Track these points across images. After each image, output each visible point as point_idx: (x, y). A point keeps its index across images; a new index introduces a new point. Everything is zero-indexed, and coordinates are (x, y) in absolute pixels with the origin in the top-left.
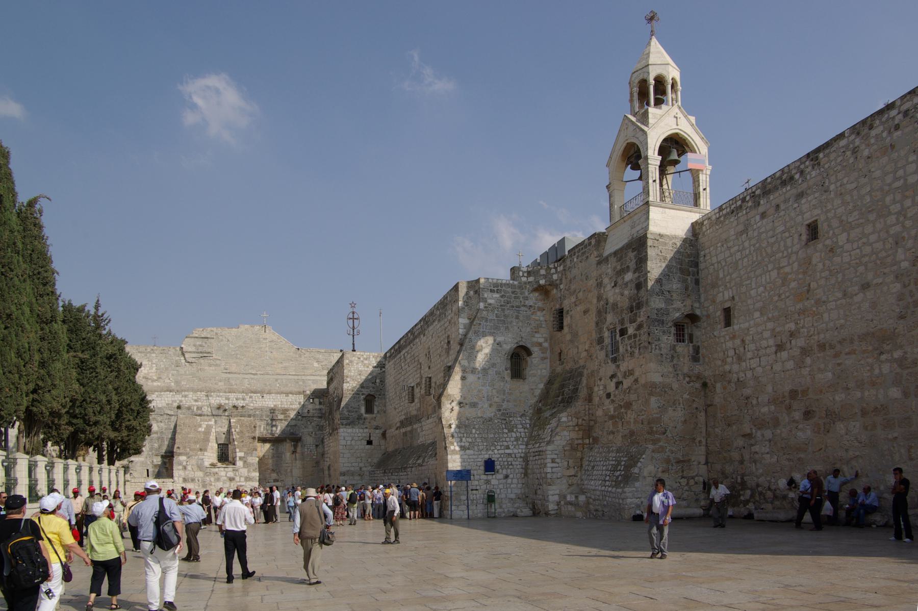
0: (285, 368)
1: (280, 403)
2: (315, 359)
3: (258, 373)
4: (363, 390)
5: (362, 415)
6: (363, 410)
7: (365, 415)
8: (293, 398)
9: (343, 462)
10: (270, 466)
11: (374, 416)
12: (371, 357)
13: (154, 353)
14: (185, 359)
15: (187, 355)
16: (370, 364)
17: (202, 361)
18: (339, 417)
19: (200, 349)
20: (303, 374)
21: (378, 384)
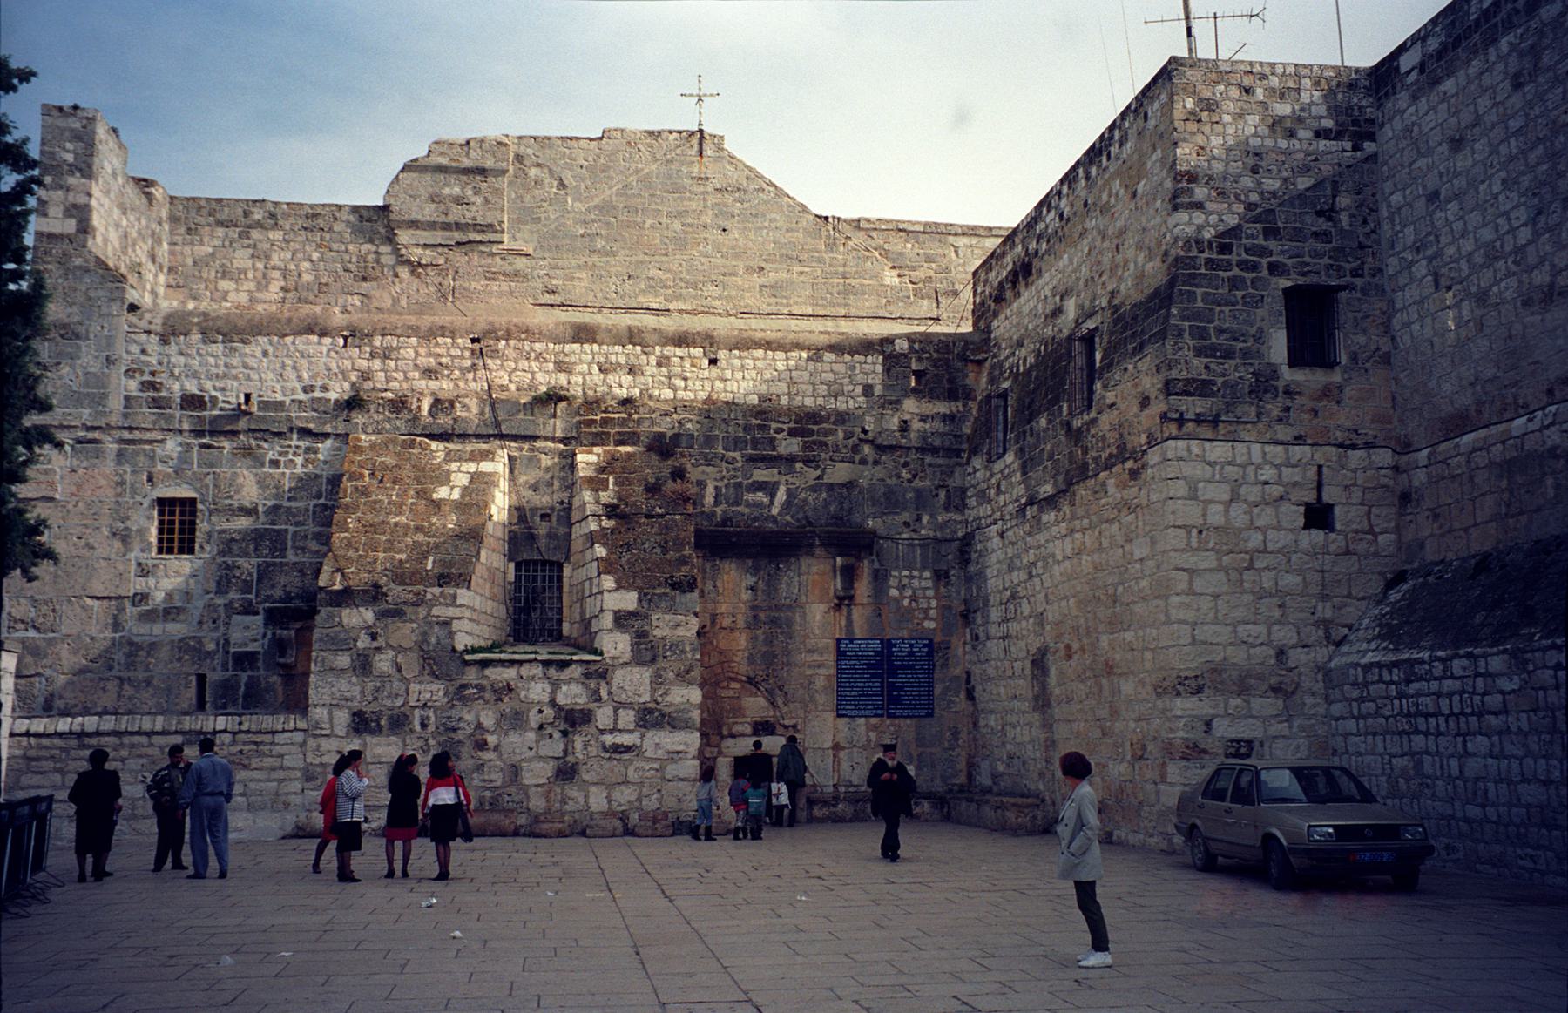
0: (775, 289)
1: (783, 387)
2: (886, 254)
3: (671, 307)
4: (1272, 245)
5: (1275, 373)
6: (1278, 346)
7: (1288, 375)
8: (839, 368)
9: (1190, 615)
10: (741, 666)
11: (1336, 377)
12: (1307, 82)
13: (276, 226)
14: (396, 251)
15: (404, 237)
16: (1300, 120)
17: (458, 258)
18: (1151, 383)
19: (454, 216)
20: (843, 312)
21: (1344, 219)
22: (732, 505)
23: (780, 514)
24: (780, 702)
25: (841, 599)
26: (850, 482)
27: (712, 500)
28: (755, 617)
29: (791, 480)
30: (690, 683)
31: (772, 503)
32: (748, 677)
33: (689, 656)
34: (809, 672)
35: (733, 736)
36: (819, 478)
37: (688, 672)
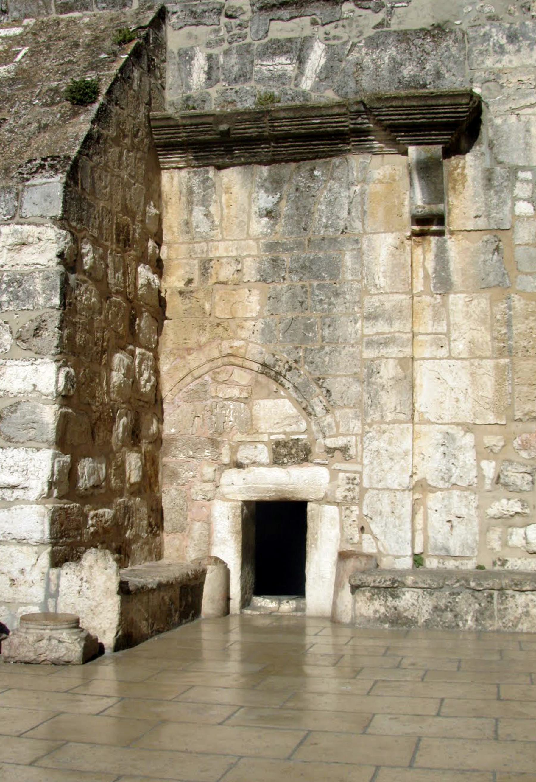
22: (236, 80)
23: (316, 88)
24: (319, 409)
25: (419, 220)
26: (438, 27)
27: (203, 77)
28: (275, 261)
29: (333, 33)
30: (40, 353)
31: (301, 72)
32: (264, 365)
33: (41, 301)
34: (369, 354)
35: (239, 466)
36: (380, 25)
37: (37, 332)
